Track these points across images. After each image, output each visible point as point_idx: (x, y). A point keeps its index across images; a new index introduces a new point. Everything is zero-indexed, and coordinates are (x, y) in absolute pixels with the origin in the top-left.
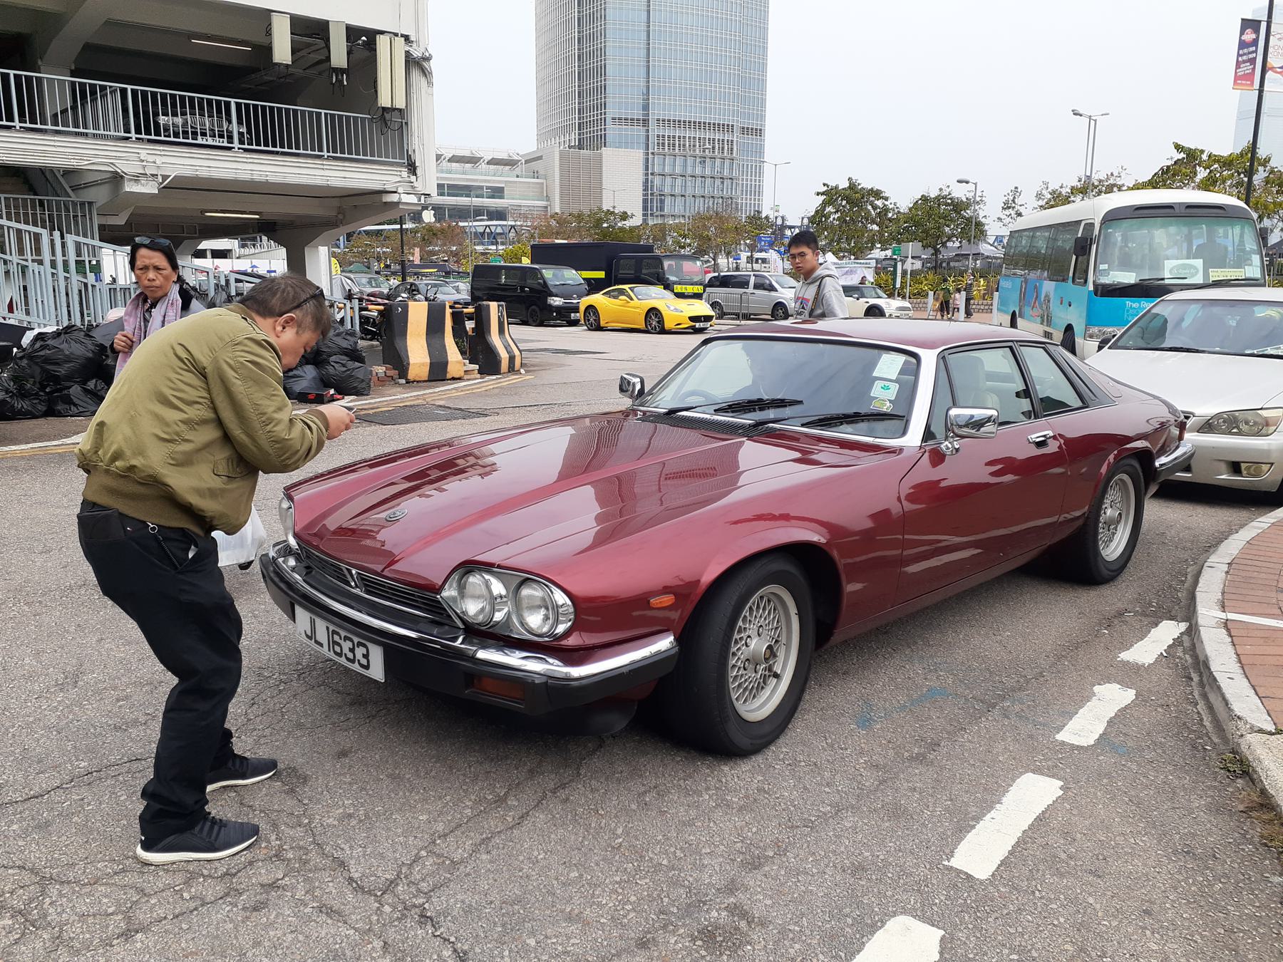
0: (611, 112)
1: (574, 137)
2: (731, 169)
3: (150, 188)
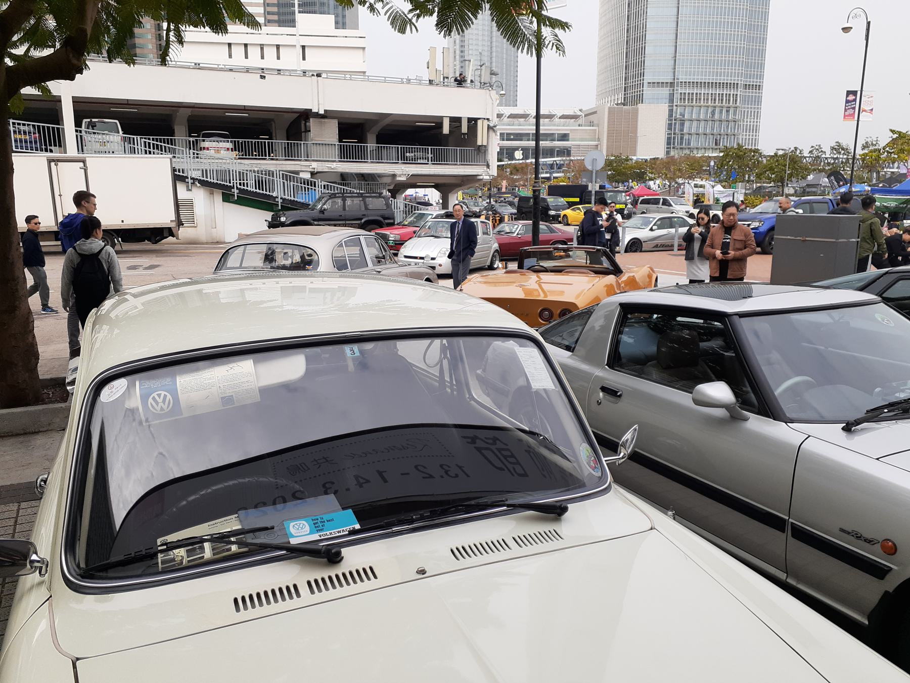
0: (648, 78)
1: (620, 97)
2: (735, 114)
3: (403, 179)
